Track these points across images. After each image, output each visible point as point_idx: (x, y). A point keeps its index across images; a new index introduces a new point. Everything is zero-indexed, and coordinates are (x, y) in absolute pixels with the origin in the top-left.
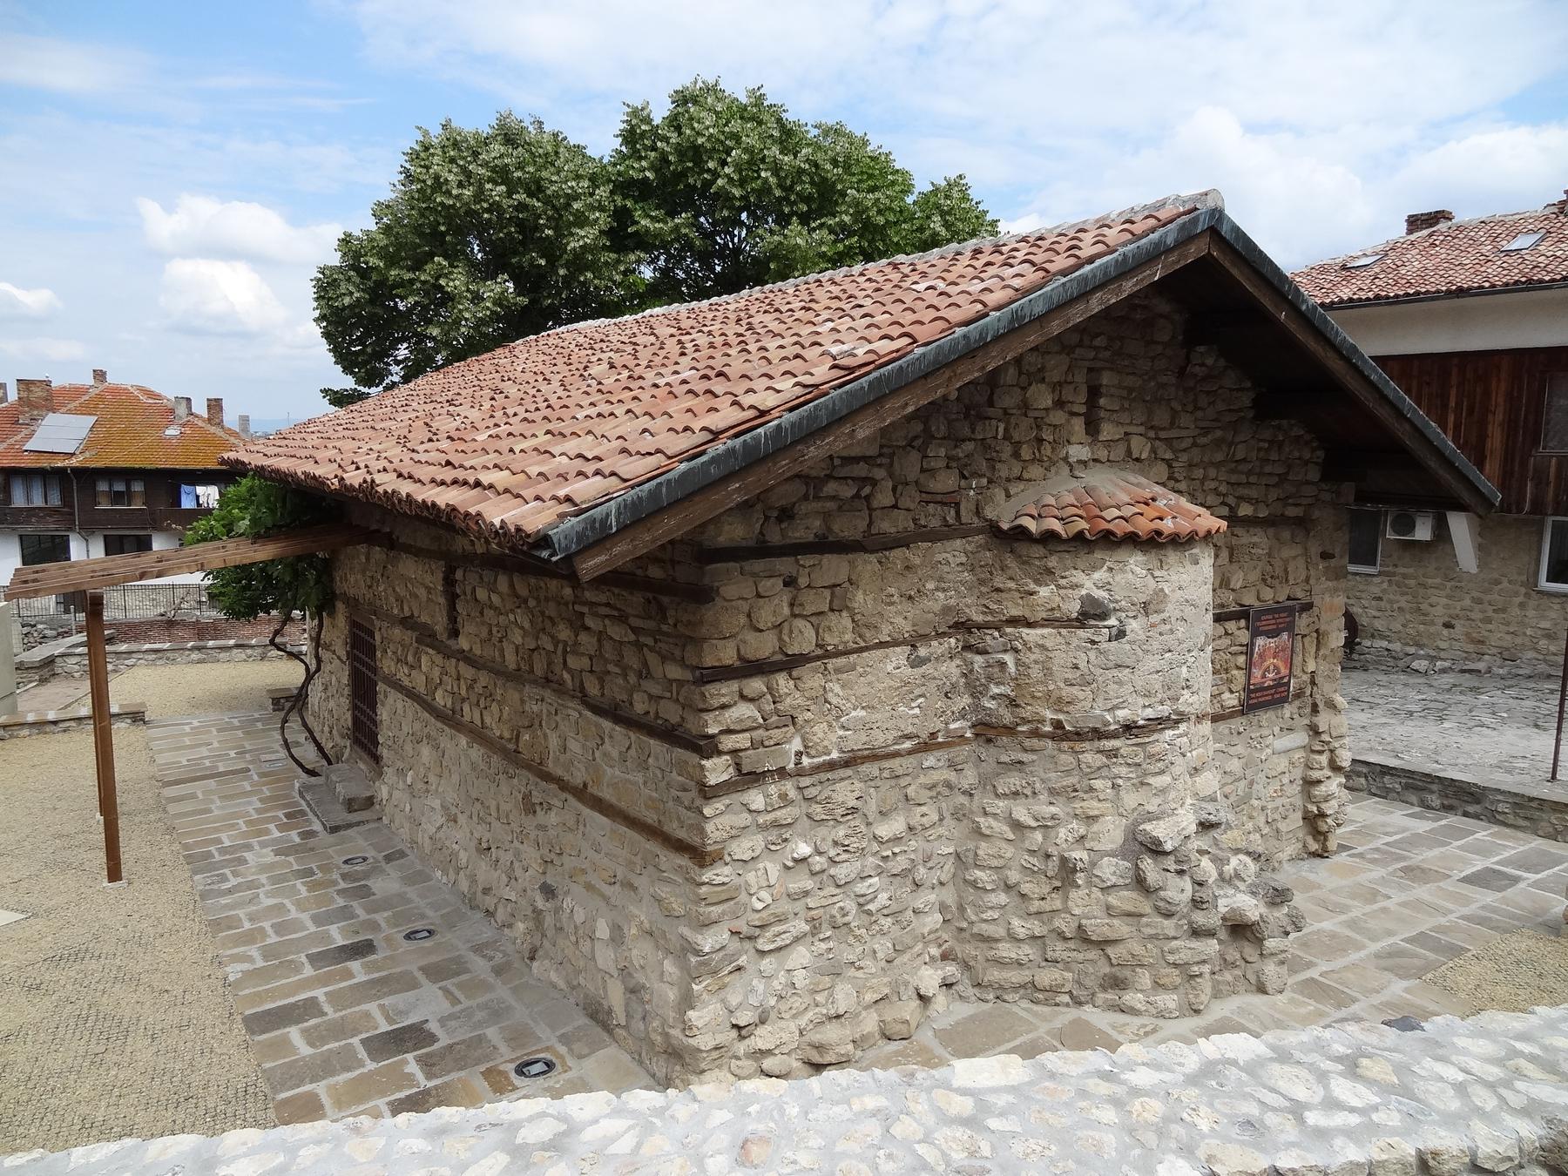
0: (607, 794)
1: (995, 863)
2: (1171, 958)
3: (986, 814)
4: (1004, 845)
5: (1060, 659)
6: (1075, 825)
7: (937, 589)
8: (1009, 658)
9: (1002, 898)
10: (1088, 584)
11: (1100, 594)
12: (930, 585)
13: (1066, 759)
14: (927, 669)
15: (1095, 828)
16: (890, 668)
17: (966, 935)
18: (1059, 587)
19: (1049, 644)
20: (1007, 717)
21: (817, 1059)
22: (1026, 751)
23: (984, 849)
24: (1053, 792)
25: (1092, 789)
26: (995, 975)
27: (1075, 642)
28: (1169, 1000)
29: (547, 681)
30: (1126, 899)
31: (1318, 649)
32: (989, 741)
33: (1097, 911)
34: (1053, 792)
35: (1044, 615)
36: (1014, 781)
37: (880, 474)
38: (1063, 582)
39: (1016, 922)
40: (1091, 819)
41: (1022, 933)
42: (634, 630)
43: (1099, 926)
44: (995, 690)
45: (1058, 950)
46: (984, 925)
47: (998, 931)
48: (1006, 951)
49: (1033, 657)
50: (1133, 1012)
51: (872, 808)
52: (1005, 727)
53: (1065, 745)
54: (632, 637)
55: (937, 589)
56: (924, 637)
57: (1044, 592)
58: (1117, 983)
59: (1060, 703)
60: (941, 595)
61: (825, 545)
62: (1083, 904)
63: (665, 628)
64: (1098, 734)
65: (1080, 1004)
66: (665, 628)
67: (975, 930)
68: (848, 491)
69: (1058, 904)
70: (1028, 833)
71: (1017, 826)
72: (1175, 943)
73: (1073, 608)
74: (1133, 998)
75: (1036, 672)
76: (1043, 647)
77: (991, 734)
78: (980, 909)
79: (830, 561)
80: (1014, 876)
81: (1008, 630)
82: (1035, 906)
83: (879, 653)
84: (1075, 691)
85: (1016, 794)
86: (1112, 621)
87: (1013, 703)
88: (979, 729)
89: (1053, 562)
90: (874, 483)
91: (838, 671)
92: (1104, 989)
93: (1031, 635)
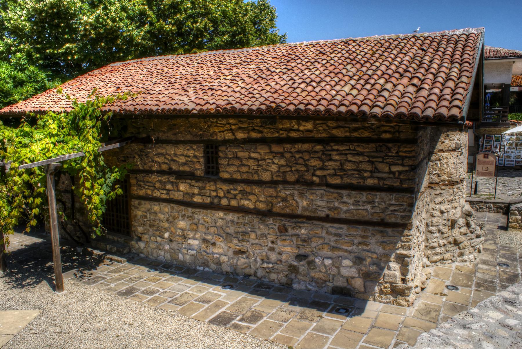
0: (343, 216)
1: (437, 224)
2: (472, 245)
3: (434, 210)
4: (438, 218)
5: (451, 161)
6: (453, 210)
8: (438, 162)
9: (437, 235)
10: (456, 139)
11: (458, 142)
13: (451, 191)
15: (457, 210)
17: (428, 248)
18: (450, 140)
19: (449, 157)
20: (437, 180)
21: (423, 287)
22: (442, 190)
23: (434, 220)
24: (449, 201)
25: (455, 199)
26: (435, 258)
27: (454, 156)
28: (472, 257)
29: (297, 182)
30: (464, 230)
32: (432, 188)
33: (458, 234)
34: (449, 201)
35: (447, 149)
36: (438, 199)
38: (451, 139)
39: (441, 241)
40: (455, 208)
41: (442, 244)
42: (368, 157)
43: (460, 238)
44: (435, 172)
45: (449, 247)
46: (433, 244)
47: (436, 245)
48: (438, 250)
49: (445, 161)
50: (465, 261)
52: (437, 183)
53: (451, 187)
54: (367, 159)
57: (447, 142)
58: (461, 255)
59: (450, 175)
62: (456, 233)
63: (390, 154)
64: (457, 183)
65: (454, 262)
66: (390, 154)
67: (431, 245)
69: (450, 234)
70: (444, 214)
71: (442, 212)
72: (473, 240)
73: (453, 146)
74: (465, 258)
75: (445, 166)
76: (446, 158)
77: (432, 186)
78: (432, 239)
80: (441, 227)
81: (439, 154)
82: (446, 235)
84: (453, 170)
85: (440, 203)
86: (460, 150)
87: (439, 176)
88: (430, 185)
89: (449, 133)
92: (459, 256)
93: (444, 155)
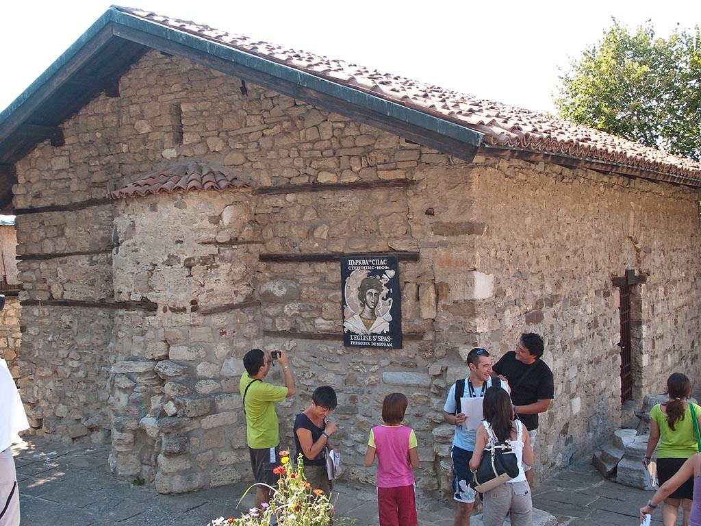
7: (100, 229)
12: (96, 227)
14: (96, 267)
16: (80, 264)
31: (437, 300)
37: (71, 176)
51: (75, 328)
55: (100, 229)
56: (97, 253)
60: (101, 232)
61: (53, 208)
68: (60, 185)
79: (56, 214)
83: (77, 256)
90: (70, 179)
91: (61, 262)
